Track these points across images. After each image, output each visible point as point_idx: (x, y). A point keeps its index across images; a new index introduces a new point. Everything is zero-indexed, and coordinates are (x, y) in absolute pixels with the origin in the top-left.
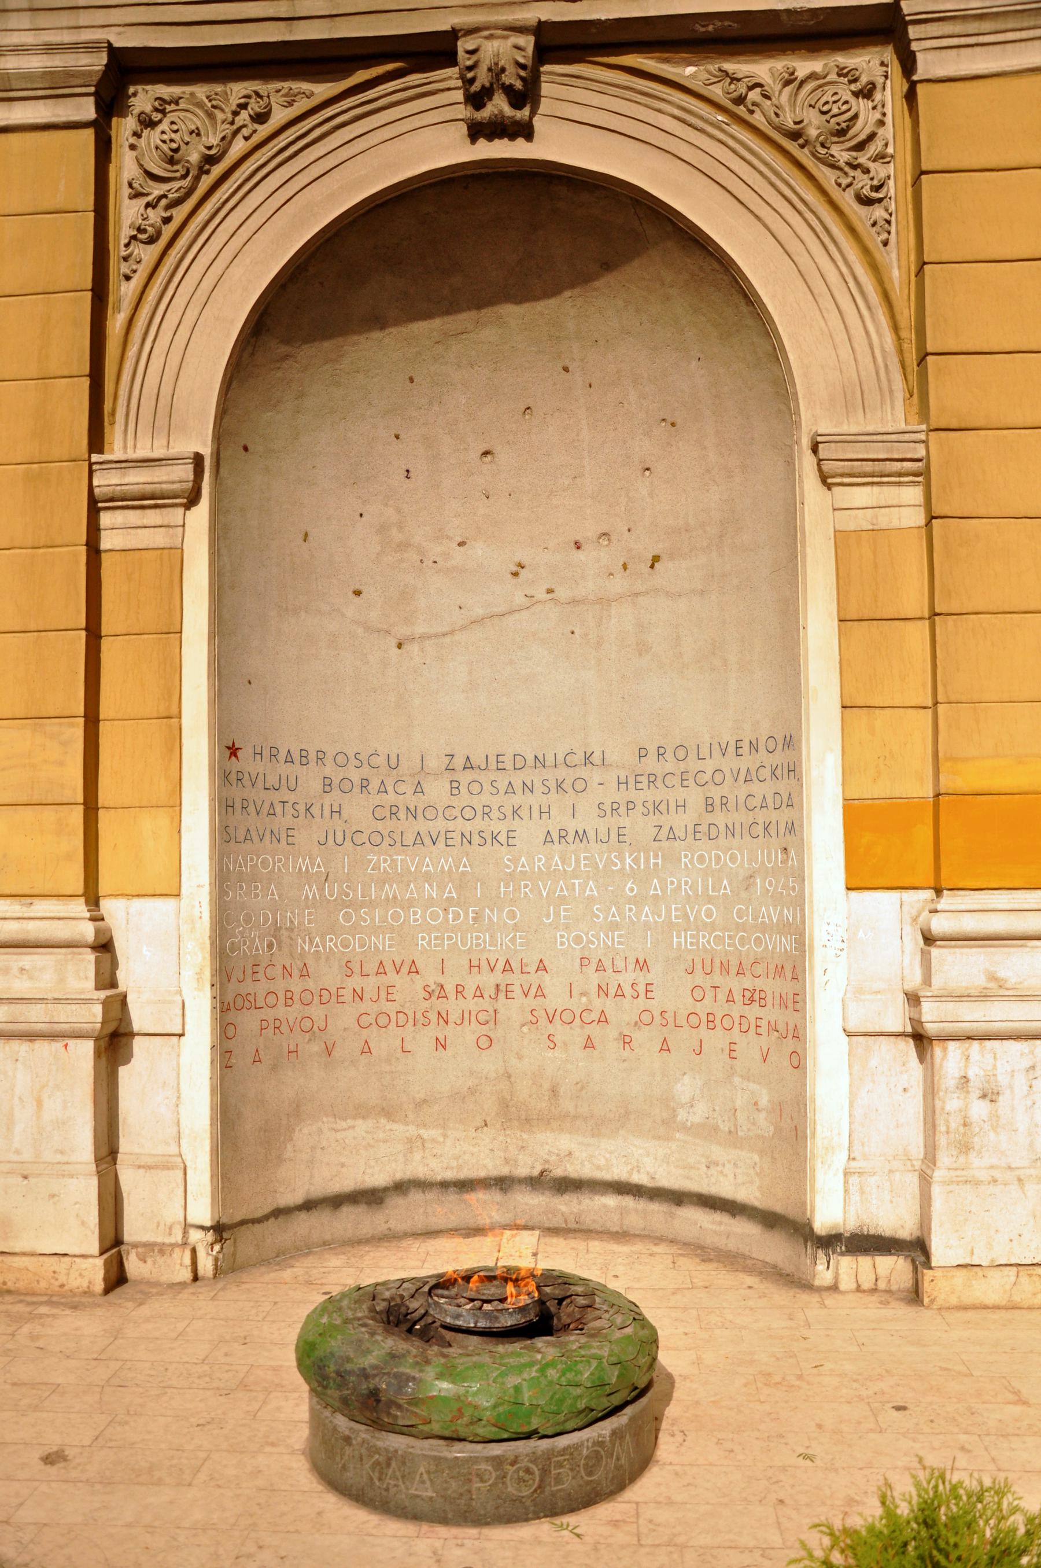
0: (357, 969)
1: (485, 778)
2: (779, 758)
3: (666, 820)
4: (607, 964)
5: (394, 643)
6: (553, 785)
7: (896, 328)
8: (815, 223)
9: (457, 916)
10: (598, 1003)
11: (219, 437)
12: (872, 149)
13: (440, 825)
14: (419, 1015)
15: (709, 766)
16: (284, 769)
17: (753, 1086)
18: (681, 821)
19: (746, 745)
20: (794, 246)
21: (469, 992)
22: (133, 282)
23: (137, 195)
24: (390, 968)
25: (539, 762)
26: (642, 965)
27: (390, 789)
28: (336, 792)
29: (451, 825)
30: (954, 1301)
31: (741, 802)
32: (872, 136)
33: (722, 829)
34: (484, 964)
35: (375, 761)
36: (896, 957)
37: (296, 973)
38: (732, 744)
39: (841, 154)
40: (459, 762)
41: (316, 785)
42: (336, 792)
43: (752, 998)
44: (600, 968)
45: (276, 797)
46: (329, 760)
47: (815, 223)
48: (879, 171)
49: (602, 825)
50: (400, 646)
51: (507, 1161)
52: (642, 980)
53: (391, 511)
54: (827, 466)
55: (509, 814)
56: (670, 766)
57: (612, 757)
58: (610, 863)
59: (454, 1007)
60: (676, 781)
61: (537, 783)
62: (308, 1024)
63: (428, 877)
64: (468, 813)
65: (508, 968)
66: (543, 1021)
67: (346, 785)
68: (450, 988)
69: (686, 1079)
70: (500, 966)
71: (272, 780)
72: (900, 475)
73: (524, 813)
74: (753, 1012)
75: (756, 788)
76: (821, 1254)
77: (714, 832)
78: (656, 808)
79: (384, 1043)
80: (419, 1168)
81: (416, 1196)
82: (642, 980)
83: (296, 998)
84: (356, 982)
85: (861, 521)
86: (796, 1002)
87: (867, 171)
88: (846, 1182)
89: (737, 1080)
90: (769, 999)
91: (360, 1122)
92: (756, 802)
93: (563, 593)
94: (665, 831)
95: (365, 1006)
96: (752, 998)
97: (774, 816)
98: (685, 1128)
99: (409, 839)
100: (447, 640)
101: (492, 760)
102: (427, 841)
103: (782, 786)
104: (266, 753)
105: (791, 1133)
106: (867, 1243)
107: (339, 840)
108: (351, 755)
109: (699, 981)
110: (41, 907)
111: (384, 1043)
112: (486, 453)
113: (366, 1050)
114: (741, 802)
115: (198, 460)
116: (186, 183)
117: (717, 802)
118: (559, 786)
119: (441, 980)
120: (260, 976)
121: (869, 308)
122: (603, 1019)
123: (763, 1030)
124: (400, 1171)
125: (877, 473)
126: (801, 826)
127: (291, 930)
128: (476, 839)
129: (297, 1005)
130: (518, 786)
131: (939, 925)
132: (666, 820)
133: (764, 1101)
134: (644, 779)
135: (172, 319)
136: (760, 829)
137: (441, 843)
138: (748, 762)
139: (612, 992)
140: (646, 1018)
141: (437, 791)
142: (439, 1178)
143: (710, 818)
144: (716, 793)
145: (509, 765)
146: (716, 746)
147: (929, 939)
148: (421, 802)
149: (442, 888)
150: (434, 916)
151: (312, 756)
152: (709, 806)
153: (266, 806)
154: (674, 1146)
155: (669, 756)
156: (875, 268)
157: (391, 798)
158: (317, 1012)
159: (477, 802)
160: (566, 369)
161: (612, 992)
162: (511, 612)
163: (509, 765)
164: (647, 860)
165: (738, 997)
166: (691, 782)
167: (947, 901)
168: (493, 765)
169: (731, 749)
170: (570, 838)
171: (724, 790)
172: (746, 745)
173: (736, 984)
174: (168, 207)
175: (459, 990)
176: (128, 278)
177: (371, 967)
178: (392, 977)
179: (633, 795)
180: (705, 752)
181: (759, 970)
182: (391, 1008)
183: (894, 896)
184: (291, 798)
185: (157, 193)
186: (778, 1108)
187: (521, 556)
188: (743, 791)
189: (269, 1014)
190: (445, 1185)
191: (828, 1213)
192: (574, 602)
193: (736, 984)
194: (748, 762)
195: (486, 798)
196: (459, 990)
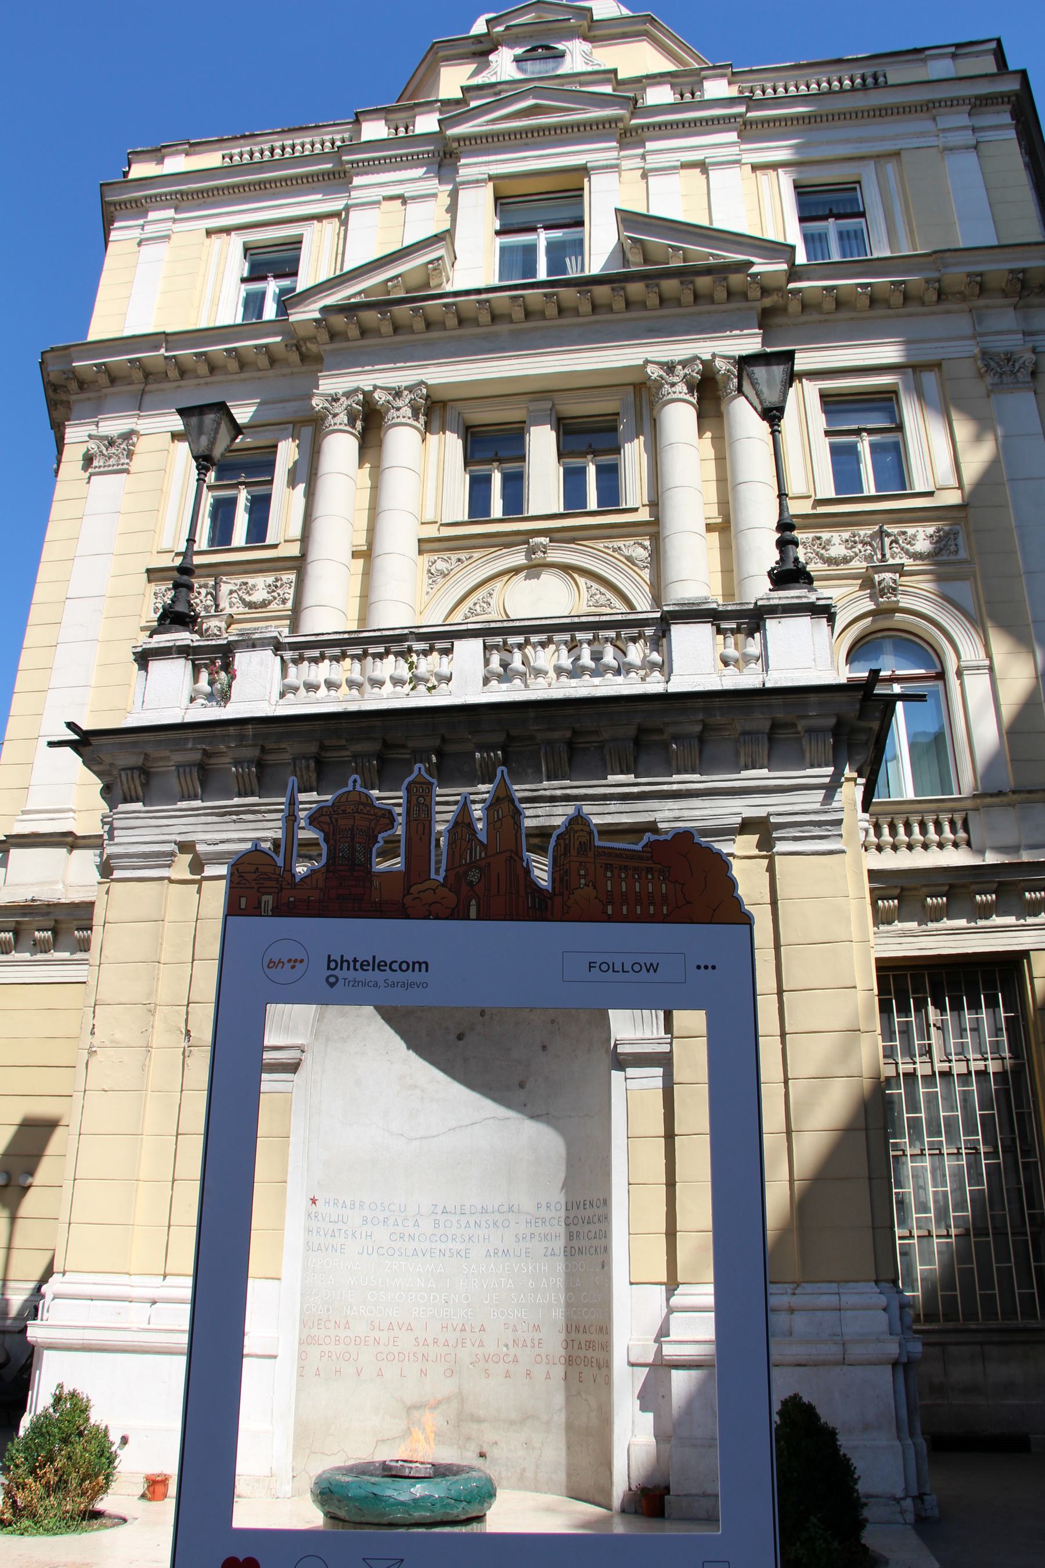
6: (491, 1222)
9: (435, 1298)
10: (512, 1351)
24: (395, 1327)
26: (537, 1328)
35: (392, 1207)
40: (439, 1210)
43: (590, 1345)
44: (515, 1330)
52: (537, 1336)
55: (467, 1239)
64: (444, 1238)
65: (463, 1330)
67: (376, 1221)
68: (430, 1341)
70: (460, 1327)
71: (334, 1218)
73: (475, 1239)
74: (590, 1353)
78: (545, 1237)
82: (537, 1336)
83: (341, 1340)
94: (550, 1250)
101: (458, 1208)
102: (420, 1254)
104: (332, 1203)
107: (370, 1252)
108: (379, 1204)
118: (495, 1224)
122: (515, 1361)
123: (594, 1364)
128: (447, 1252)
130: (472, 1223)
136: (593, 1250)
137: (428, 1255)
139: (520, 1345)
145: (467, 1211)
151: (357, 1204)
155: (552, 1207)
161: (520, 1345)
164: (540, 1268)
165: (583, 1346)
168: (458, 1211)
170: (500, 1254)
172: (588, 1203)
175: (435, 1342)
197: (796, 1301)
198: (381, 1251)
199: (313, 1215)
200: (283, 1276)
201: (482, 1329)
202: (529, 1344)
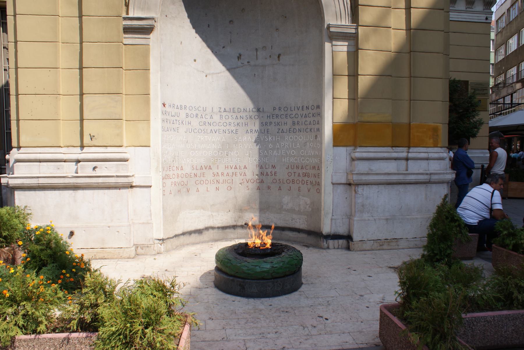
2: (315, 111)
4: (264, 166)
5: (205, 75)
6: (248, 117)
9: (222, 153)
14: (212, 181)
16: (176, 110)
17: (305, 198)
18: (285, 128)
19: (305, 107)
21: (225, 175)
24: (204, 168)
26: (274, 167)
27: (204, 117)
28: (189, 117)
29: (220, 128)
30: (359, 249)
31: (303, 123)
33: (298, 130)
34: (229, 167)
35: (200, 109)
37: (180, 169)
38: (301, 107)
40: (222, 110)
41: (185, 116)
42: (189, 117)
43: (305, 175)
46: (188, 108)
50: (206, 76)
51: (235, 221)
52: (274, 171)
56: (283, 112)
58: (265, 139)
59: (221, 178)
60: (284, 116)
62: (182, 183)
64: (225, 124)
66: (246, 182)
67: (192, 116)
68: (220, 174)
71: (173, 114)
72: (350, 37)
73: (240, 124)
74: (306, 179)
75: (308, 119)
76: (325, 240)
82: (274, 171)
86: (319, 176)
88: (331, 222)
89: (301, 197)
90: (311, 175)
92: (308, 123)
93: (252, 63)
94: (281, 130)
95: (197, 178)
96: (305, 175)
97: (313, 126)
99: (209, 131)
100: (219, 75)
102: (214, 132)
103: (316, 119)
105: (316, 210)
106: (336, 237)
107: (190, 131)
109: (290, 171)
110: (110, 149)
112: (230, 21)
113: (198, 191)
114: (303, 123)
117: (296, 122)
118: (250, 117)
119: (217, 171)
120: (171, 169)
123: (309, 183)
126: (322, 129)
127: (178, 156)
128: (227, 132)
130: (239, 117)
131: (357, 155)
133: (309, 202)
136: (309, 130)
137: (217, 132)
138: (305, 112)
139: (265, 174)
140: (275, 181)
141: (216, 118)
142: (217, 226)
143: (294, 127)
144: (296, 120)
146: (296, 108)
151: (183, 107)
152: (294, 123)
153: (172, 121)
155: (282, 110)
157: (204, 119)
161: (265, 174)
162: (237, 68)
163: (236, 111)
164: (275, 138)
165: (301, 175)
166: (289, 117)
167: (359, 149)
169: (301, 108)
170: (253, 132)
172: (305, 107)
173: (301, 172)
175: (222, 174)
177: (199, 167)
178: (204, 170)
179: (271, 120)
181: (308, 168)
182: (204, 179)
184: (178, 119)
188: (304, 120)
189: (173, 180)
191: (326, 229)
193: (301, 172)
194: (305, 112)
195: (230, 120)
196: (222, 174)
197: (410, 155)
198: (196, 131)
199: (164, 113)
200: (151, 145)
201: (245, 167)
202: (269, 174)
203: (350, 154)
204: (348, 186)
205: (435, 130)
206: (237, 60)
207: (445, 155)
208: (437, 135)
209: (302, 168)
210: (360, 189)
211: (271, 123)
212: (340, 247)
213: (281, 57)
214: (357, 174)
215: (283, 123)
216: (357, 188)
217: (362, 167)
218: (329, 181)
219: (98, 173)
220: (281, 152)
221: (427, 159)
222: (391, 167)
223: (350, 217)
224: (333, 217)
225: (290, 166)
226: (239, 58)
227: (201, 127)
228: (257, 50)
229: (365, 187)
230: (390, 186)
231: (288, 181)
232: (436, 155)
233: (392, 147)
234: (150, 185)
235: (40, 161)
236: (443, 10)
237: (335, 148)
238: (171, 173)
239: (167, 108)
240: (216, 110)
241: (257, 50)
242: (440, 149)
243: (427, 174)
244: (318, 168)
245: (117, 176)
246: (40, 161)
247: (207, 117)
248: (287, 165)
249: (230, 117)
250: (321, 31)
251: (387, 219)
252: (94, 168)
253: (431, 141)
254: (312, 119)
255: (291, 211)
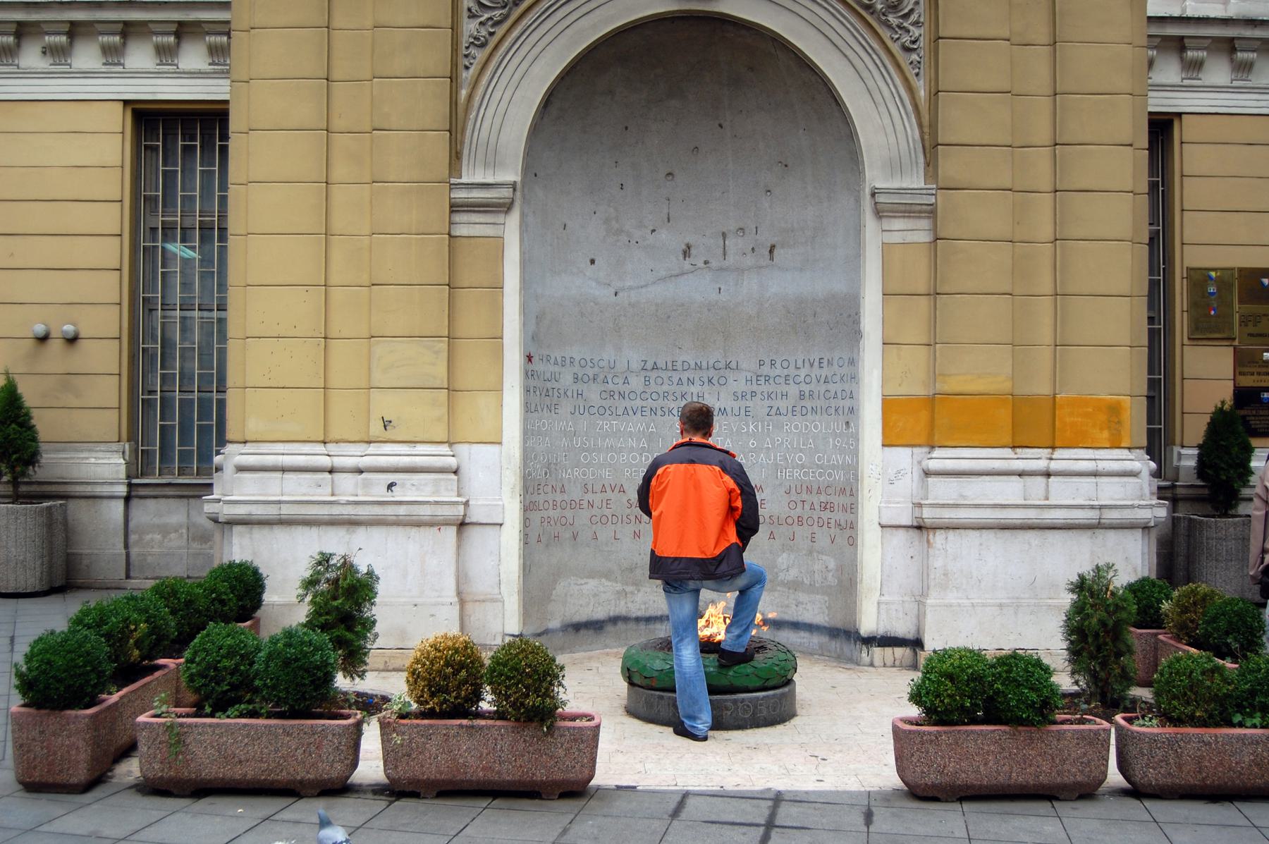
0: (590, 487)
1: (664, 375)
3: (776, 404)
5: (613, 291)
6: (706, 380)
7: (920, 126)
8: (878, 62)
11: (527, 169)
12: (913, 18)
13: (638, 403)
15: (803, 373)
17: (824, 557)
20: (865, 74)
22: (471, 70)
23: (472, 16)
24: (608, 489)
25: (698, 367)
29: (644, 404)
32: (912, 11)
35: (601, 364)
36: (909, 484)
39: (892, 19)
40: (649, 365)
43: (825, 507)
45: (549, 385)
46: (576, 363)
47: (878, 62)
48: (916, 32)
49: (736, 405)
53: (612, 210)
54: (879, 207)
57: (744, 365)
61: (697, 379)
63: (631, 434)
67: (586, 379)
69: (785, 555)
71: (548, 375)
72: (920, 212)
74: (826, 515)
75: (832, 387)
76: (864, 648)
77: (804, 411)
79: (605, 534)
80: (621, 608)
81: (621, 625)
84: (590, 497)
85: (896, 238)
86: (852, 508)
87: (908, 31)
91: (590, 581)
93: (714, 264)
95: (595, 511)
96: (825, 507)
97: (841, 403)
98: (783, 584)
99: (620, 412)
101: (670, 365)
102: (631, 413)
103: (846, 387)
105: (846, 585)
110: (421, 449)
111: (605, 534)
112: (669, 174)
115: (514, 186)
116: (504, 11)
121: (907, 114)
123: (832, 525)
124: (613, 611)
125: (908, 211)
128: (659, 412)
129: (559, 510)
130: (685, 380)
131: (933, 465)
132: (776, 404)
133: (832, 564)
134: (762, 379)
135: (497, 95)
136: (833, 410)
141: (636, 383)
143: (803, 403)
144: (806, 388)
145: (679, 367)
147: (927, 473)
148: (626, 389)
149: (639, 440)
150: (634, 458)
151: (568, 361)
152: (802, 396)
154: (776, 594)
155: (778, 365)
156: (911, 90)
157: (611, 386)
158: (569, 513)
159: (661, 389)
160: (721, 126)
162: (683, 274)
165: (817, 507)
167: (937, 453)
169: (816, 364)
171: (812, 387)
173: (816, 500)
174: (494, 25)
176: (467, 68)
177: (598, 488)
178: (609, 494)
180: (800, 363)
182: (608, 512)
183: (908, 451)
184: (556, 385)
185: (486, 16)
186: (840, 568)
187: (690, 239)
188: (823, 388)
189: (545, 514)
190: (638, 620)
191: (869, 624)
192: (721, 269)
193: (816, 500)
197: (1054, 466)
200: (505, 440)
203: (920, 463)
204: (914, 534)
205: (1114, 410)
206: (681, 257)
207: (1136, 465)
208: (1119, 422)
209: (819, 492)
210: (939, 538)
211: (753, 394)
212: (897, 663)
213: (776, 252)
214: (932, 506)
215: (779, 396)
216: (931, 536)
217: (943, 490)
218: (876, 521)
219: (398, 494)
220: (775, 457)
221: (1095, 474)
222: (1010, 490)
223: (920, 601)
224: (883, 598)
225: (793, 487)
226: (686, 253)
227: (604, 403)
228: (724, 235)
229: (951, 533)
230: (1007, 533)
231: (790, 521)
232: (1116, 466)
233: (1014, 447)
234: (500, 521)
235: (284, 470)
236: (1131, 145)
237: (886, 449)
238: (541, 498)
239: (538, 366)
240: (635, 365)
241: (724, 235)
242: (1126, 451)
243: (1092, 507)
244: (850, 491)
245: (437, 503)
246: (284, 470)
247: (616, 380)
248: (787, 484)
249: (666, 380)
250: (858, 201)
251: (1001, 606)
252: (390, 486)
253: (1106, 434)
254: (837, 387)
255: (795, 585)
